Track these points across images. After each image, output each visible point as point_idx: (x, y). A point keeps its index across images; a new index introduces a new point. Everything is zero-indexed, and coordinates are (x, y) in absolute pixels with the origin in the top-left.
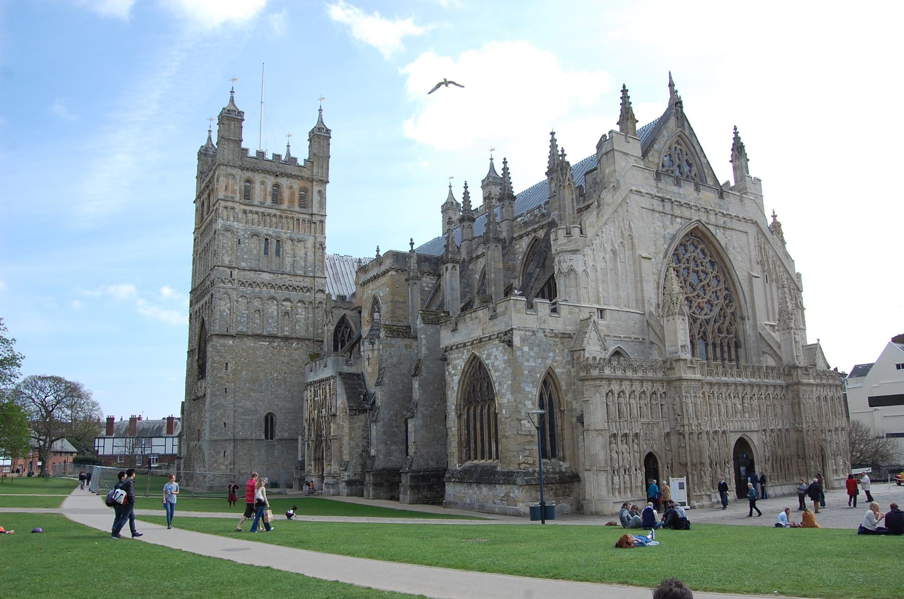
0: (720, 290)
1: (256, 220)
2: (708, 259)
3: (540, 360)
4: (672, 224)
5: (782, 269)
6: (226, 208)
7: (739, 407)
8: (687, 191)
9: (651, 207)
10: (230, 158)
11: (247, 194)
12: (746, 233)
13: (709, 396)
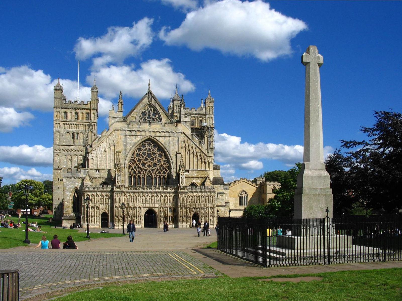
0: (162, 159)
1: (68, 127)
2: (156, 148)
3: (72, 186)
4: (136, 138)
5: (197, 149)
6: (57, 124)
7: (148, 199)
8: (145, 126)
9: (125, 134)
10: (58, 105)
11: (66, 118)
12: (178, 137)
13: (134, 196)
